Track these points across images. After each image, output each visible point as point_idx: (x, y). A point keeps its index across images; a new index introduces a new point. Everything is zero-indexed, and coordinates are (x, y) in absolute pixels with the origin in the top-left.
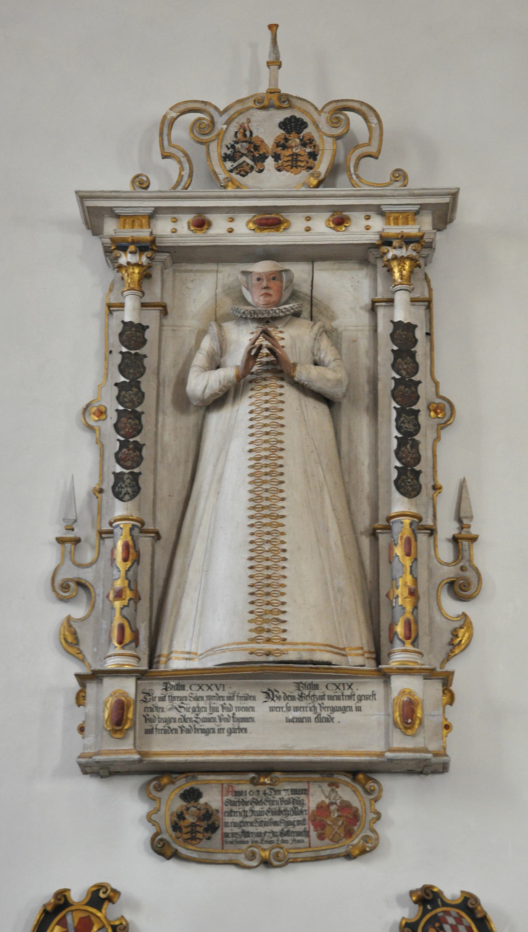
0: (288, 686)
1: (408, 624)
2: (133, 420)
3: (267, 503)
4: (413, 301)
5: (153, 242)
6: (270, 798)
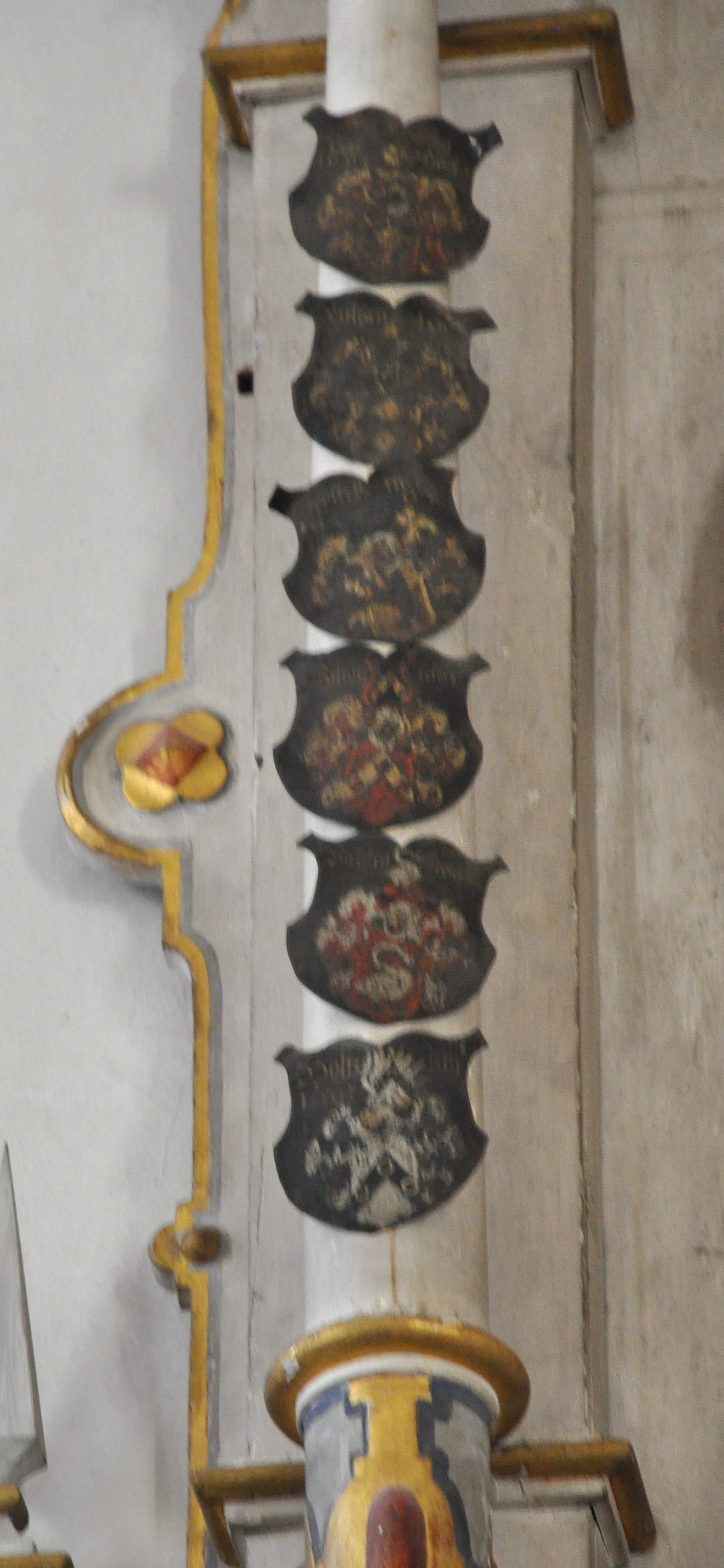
2: (411, 713)
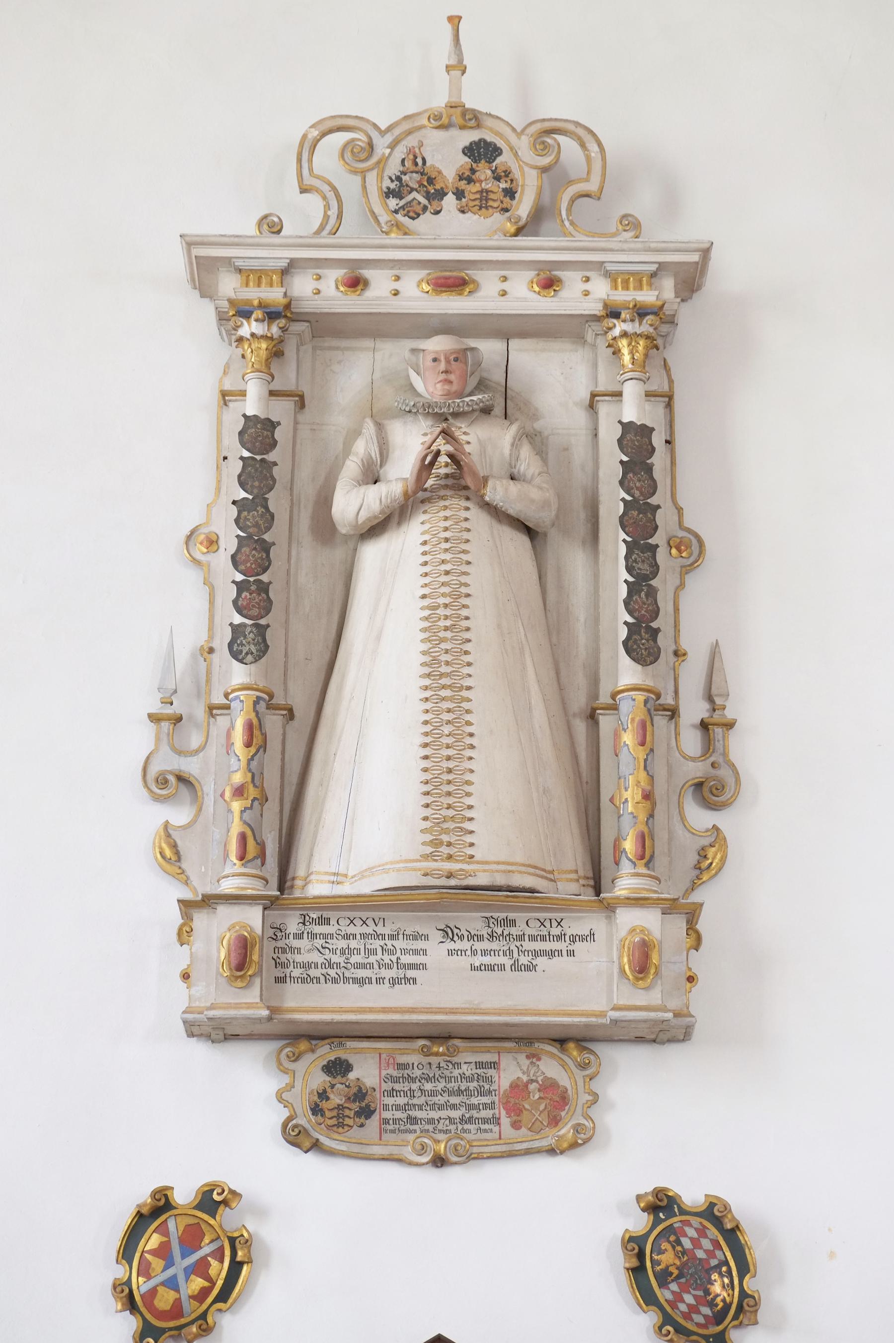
0: (473, 922)
1: (642, 839)
3: (449, 669)
4: (649, 395)
5: (288, 306)
6: (447, 1073)
